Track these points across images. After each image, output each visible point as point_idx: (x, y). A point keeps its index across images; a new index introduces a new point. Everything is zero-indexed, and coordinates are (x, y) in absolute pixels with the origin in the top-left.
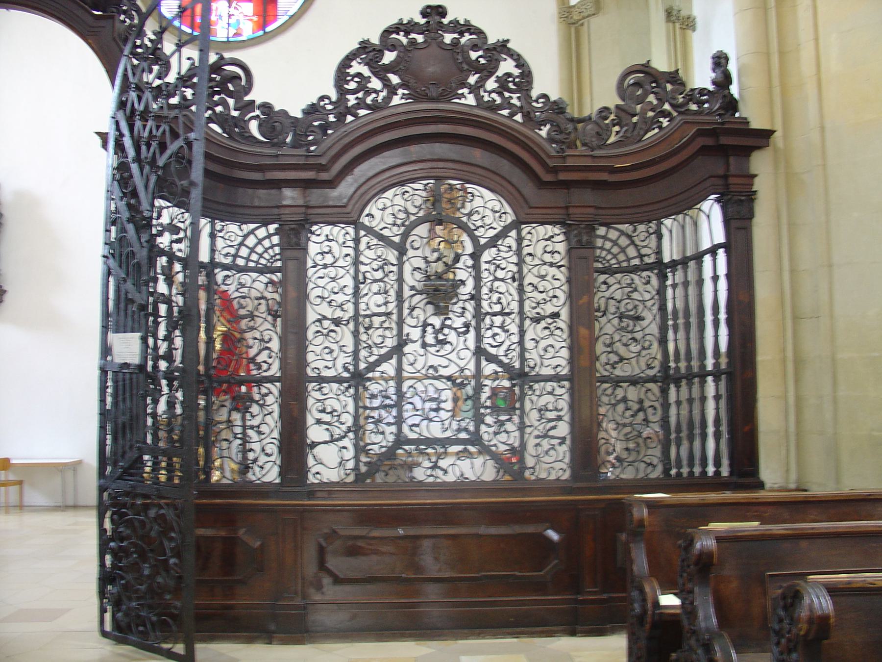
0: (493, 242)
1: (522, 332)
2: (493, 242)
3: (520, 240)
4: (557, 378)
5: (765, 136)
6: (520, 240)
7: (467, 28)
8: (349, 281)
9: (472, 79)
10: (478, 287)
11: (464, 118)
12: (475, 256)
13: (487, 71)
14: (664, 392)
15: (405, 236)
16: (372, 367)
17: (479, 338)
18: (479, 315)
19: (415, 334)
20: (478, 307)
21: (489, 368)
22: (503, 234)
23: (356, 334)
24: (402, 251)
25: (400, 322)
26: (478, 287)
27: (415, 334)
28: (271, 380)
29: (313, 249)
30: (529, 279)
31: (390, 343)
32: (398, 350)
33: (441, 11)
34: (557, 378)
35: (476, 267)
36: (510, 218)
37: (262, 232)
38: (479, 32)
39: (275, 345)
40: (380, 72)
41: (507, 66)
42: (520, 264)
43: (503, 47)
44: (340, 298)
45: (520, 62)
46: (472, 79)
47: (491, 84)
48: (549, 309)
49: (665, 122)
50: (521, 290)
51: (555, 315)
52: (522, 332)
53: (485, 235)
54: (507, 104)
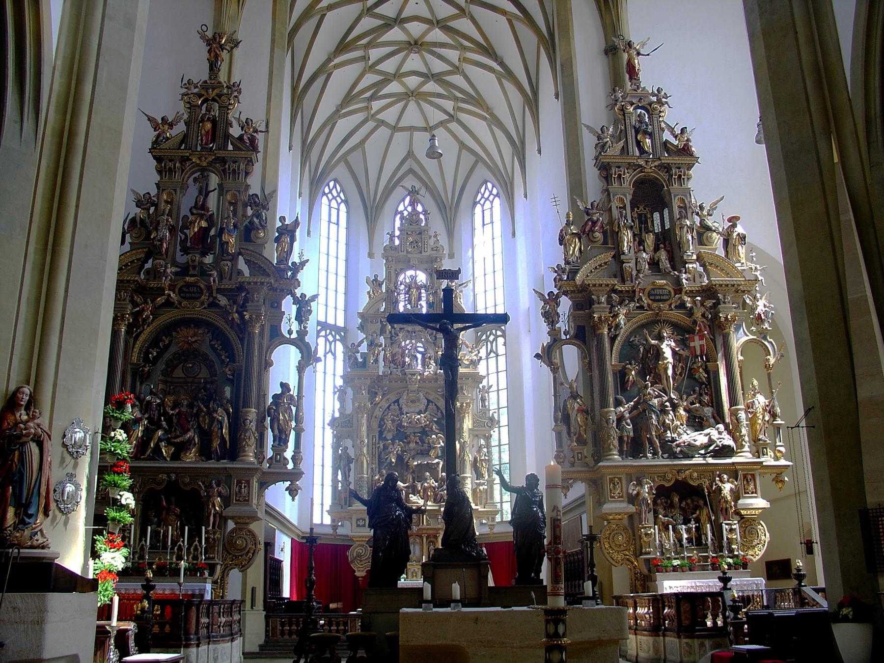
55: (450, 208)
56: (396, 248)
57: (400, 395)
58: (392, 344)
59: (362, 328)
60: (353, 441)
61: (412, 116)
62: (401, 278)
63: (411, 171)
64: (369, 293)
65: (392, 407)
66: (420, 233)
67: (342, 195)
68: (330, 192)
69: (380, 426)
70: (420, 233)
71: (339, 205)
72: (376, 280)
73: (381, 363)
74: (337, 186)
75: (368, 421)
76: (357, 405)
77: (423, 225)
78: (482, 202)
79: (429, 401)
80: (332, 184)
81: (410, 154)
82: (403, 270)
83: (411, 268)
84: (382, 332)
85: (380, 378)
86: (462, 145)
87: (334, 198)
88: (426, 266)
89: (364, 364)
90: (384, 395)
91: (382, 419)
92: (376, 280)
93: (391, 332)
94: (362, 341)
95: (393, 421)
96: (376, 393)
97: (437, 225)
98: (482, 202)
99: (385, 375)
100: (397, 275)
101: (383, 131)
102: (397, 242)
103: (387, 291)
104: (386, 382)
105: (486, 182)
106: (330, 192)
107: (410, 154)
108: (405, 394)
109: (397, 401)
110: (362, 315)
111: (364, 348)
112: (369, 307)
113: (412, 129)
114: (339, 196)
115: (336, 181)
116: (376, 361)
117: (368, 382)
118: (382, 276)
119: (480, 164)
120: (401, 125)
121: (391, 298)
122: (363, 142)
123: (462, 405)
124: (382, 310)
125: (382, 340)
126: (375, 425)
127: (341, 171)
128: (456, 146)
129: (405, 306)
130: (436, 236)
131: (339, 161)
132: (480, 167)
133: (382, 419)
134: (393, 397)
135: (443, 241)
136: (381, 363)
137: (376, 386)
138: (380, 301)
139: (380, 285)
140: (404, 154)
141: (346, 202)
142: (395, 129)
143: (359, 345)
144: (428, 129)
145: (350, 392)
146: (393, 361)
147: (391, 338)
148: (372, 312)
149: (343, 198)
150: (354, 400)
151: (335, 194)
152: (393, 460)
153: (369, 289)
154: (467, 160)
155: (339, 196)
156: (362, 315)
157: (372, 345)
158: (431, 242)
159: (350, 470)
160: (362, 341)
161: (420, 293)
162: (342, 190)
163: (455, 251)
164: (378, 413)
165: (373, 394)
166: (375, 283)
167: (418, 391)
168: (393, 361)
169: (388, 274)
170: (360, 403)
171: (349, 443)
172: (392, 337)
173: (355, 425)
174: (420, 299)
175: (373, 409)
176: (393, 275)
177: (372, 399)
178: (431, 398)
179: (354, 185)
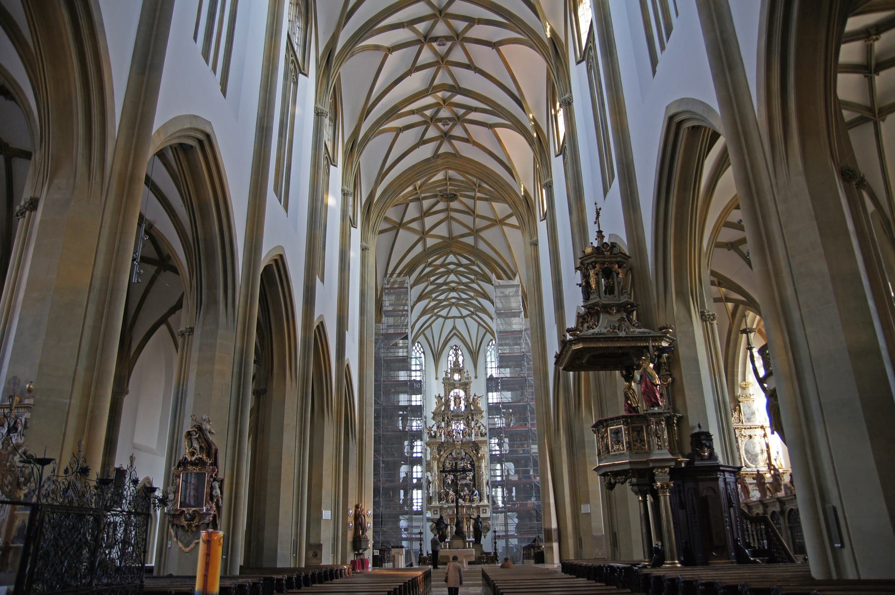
55: (475, 353)
56: (449, 379)
57: (452, 451)
58: (448, 426)
59: (433, 418)
60: (431, 473)
61: (454, 312)
62: (452, 393)
63: (455, 334)
64: (436, 402)
65: (449, 456)
66: (460, 371)
67: (421, 349)
68: (416, 348)
69: (443, 466)
70: (460, 371)
71: (420, 354)
72: (439, 396)
73: (443, 436)
74: (419, 344)
75: (438, 463)
76: (432, 456)
77: (461, 366)
78: (490, 350)
79: (466, 453)
80: (416, 344)
81: (454, 328)
82: (452, 389)
83: (456, 388)
84: (443, 420)
85: (442, 442)
86: (479, 324)
87: (418, 351)
88: (463, 387)
89: (435, 436)
90: (444, 451)
91: (444, 462)
92: (439, 396)
93: (447, 421)
94: (433, 425)
95: (449, 463)
96: (441, 450)
97: (469, 367)
98: (490, 350)
99: (445, 442)
100: (449, 392)
101: (441, 320)
102: (449, 375)
103: (445, 400)
104: (445, 445)
105: (492, 340)
106: (416, 348)
107: (454, 328)
108: (455, 450)
109: (451, 454)
110: (433, 413)
111: (435, 429)
112: (437, 409)
113: (454, 317)
114: (420, 350)
115: (418, 342)
116: (441, 435)
117: (437, 446)
118: (442, 395)
119: (488, 333)
120: (450, 315)
121: (447, 404)
122: (430, 325)
123: (481, 456)
124: (443, 409)
125: (443, 424)
126: (441, 466)
127: (421, 338)
128: (477, 324)
129: (454, 407)
130: (467, 372)
131: (421, 333)
132: (488, 335)
133: (444, 462)
134: (448, 452)
135: (472, 374)
136: (443, 436)
137: (441, 447)
138: (442, 406)
139: (441, 399)
140: (451, 328)
141: (424, 352)
142: (446, 318)
143: (432, 427)
144: (463, 317)
145: (428, 449)
146: (449, 435)
147: (447, 423)
148: (438, 411)
149: (422, 351)
150: (431, 454)
151: (418, 349)
152: (450, 482)
153: (436, 401)
154: (482, 331)
155: (420, 350)
156: (433, 413)
157: (438, 427)
158: (465, 375)
159: (430, 487)
160: (433, 425)
161: (460, 401)
162: (422, 347)
163: (478, 375)
164: (442, 459)
165: (439, 451)
166: (439, 398)
167: (461, 449)
168: (449, 435)
169: (445, 392)
170: (434, 456)
171: (429, 474)
172: (448, 423)
173: (431, 466)
174: (460, 403)
175: (440, 458)
176: (448, 390)
177: (439, 454)
178: (467, 452)
179: (427, 344)
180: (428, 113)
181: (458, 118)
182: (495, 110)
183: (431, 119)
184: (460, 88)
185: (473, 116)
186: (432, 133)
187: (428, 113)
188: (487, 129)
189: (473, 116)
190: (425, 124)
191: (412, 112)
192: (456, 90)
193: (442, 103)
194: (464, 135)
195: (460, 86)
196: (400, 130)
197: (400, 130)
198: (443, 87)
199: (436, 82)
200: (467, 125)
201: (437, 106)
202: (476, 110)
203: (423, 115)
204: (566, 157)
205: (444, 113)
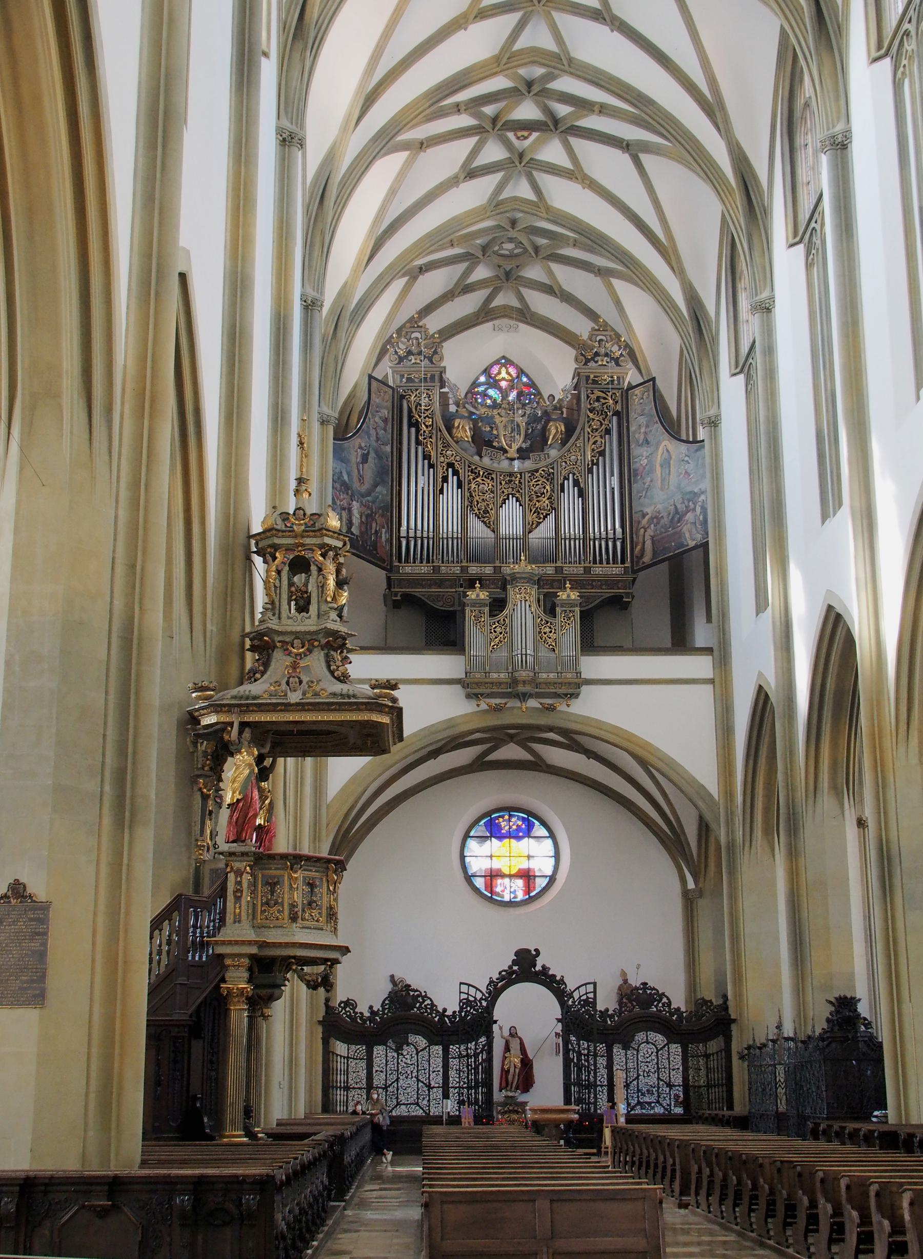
0: (661, 1049)
1: (670, 1074)
2: (661, 1049)
3: (668, 1048)
4: (679, 1086)
5: (734, 1021)
6: (668, 1048)
7: (654, 989)
8: (624, 1059)
9: (655, 1003)
10: (658, 1061)
11: (652, 1015)
12: (657, 1053)
13: (659, 1001)
14: (708, 1090)
15: (639, 1047)
16: (631, 1082)
17: (658, 1075)
18: (658, 1068)
19: (642, 1074)
20: (658, 1066)
21: (661, 1083)
22: (664, 1046)
23: (626, 1074)
24: (638, 1051)
25: (638, 1070)
26: (658, 1061)
27: (642, 1074)
28: (605, 1086)
29: (615, 1050)
30: (671, 1059)
31: (635, 1076)
32: (637, 1078)
33: (646, 984)
34: (679, 1086)
35: (657, 1056)
36: (666, 1042)
37: (601, 1046)
38: (658, 991)
39: (605, 1076)
40: (631, 1001)
41: (665, 1000)
42: (669, 1055)
43: (663, 994)
44: (622, 1064)
45: (668, 999)
46: (655, 1003)
47: (660, 1005)
48: (677, 1067)
49: (708, 1015)
50: (669, 1062)
51: (678, 1069)
52: (670, 1074)
53: (659, 1047)
54: (664, 1010)
180: (489, 110)
181: (556, 121)
182: (644, 115)
183: (494, 120)
184: (571, 60)
185: (593, 122)
186: (493, 152)
187: (489, 110)
188: (621, 152)
189: (593, 122)
190: (476, 134)
191: (457, 108)
192: (564, 65)
193: (523, 89)
194: (566, 163)
195: (572, 55)
196: (423, 145)
197: (423, 145)
198: (535, 55)
199: (518, 46)
200: (574, 141)
201: (513, 95)
202: (603, 110)
203: (478, 115)
204: (814, 251)
205: (527, 111)
